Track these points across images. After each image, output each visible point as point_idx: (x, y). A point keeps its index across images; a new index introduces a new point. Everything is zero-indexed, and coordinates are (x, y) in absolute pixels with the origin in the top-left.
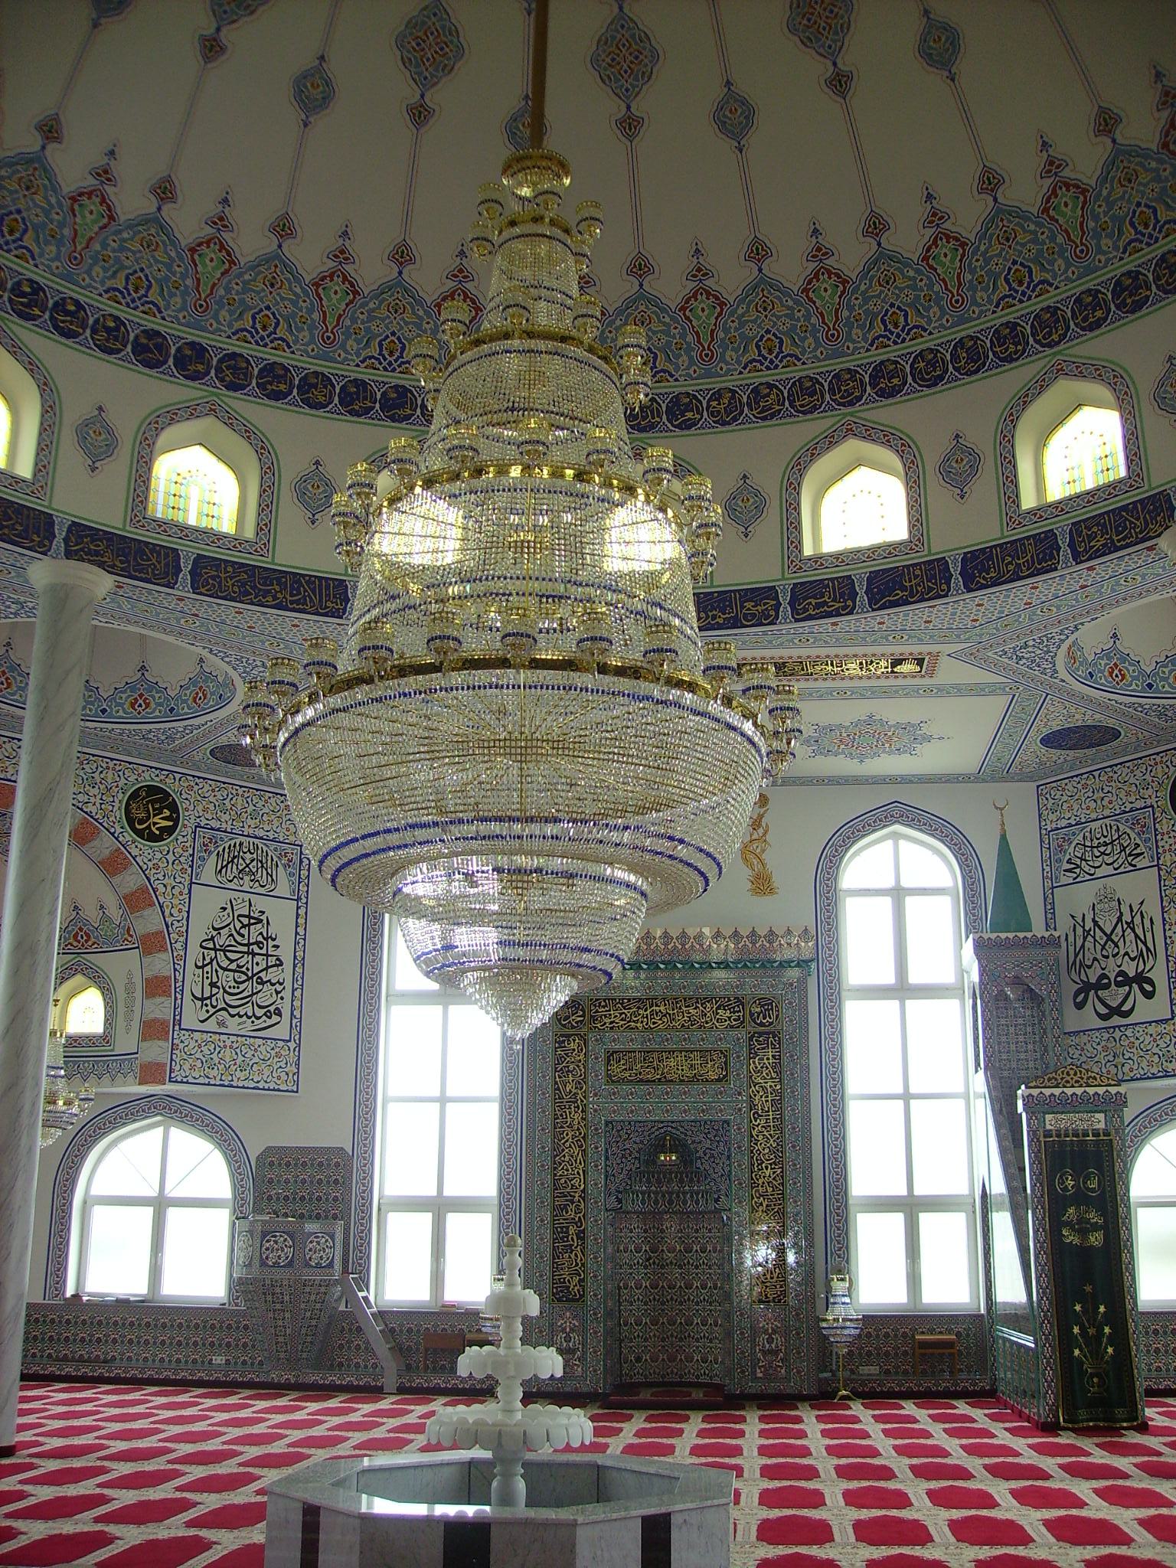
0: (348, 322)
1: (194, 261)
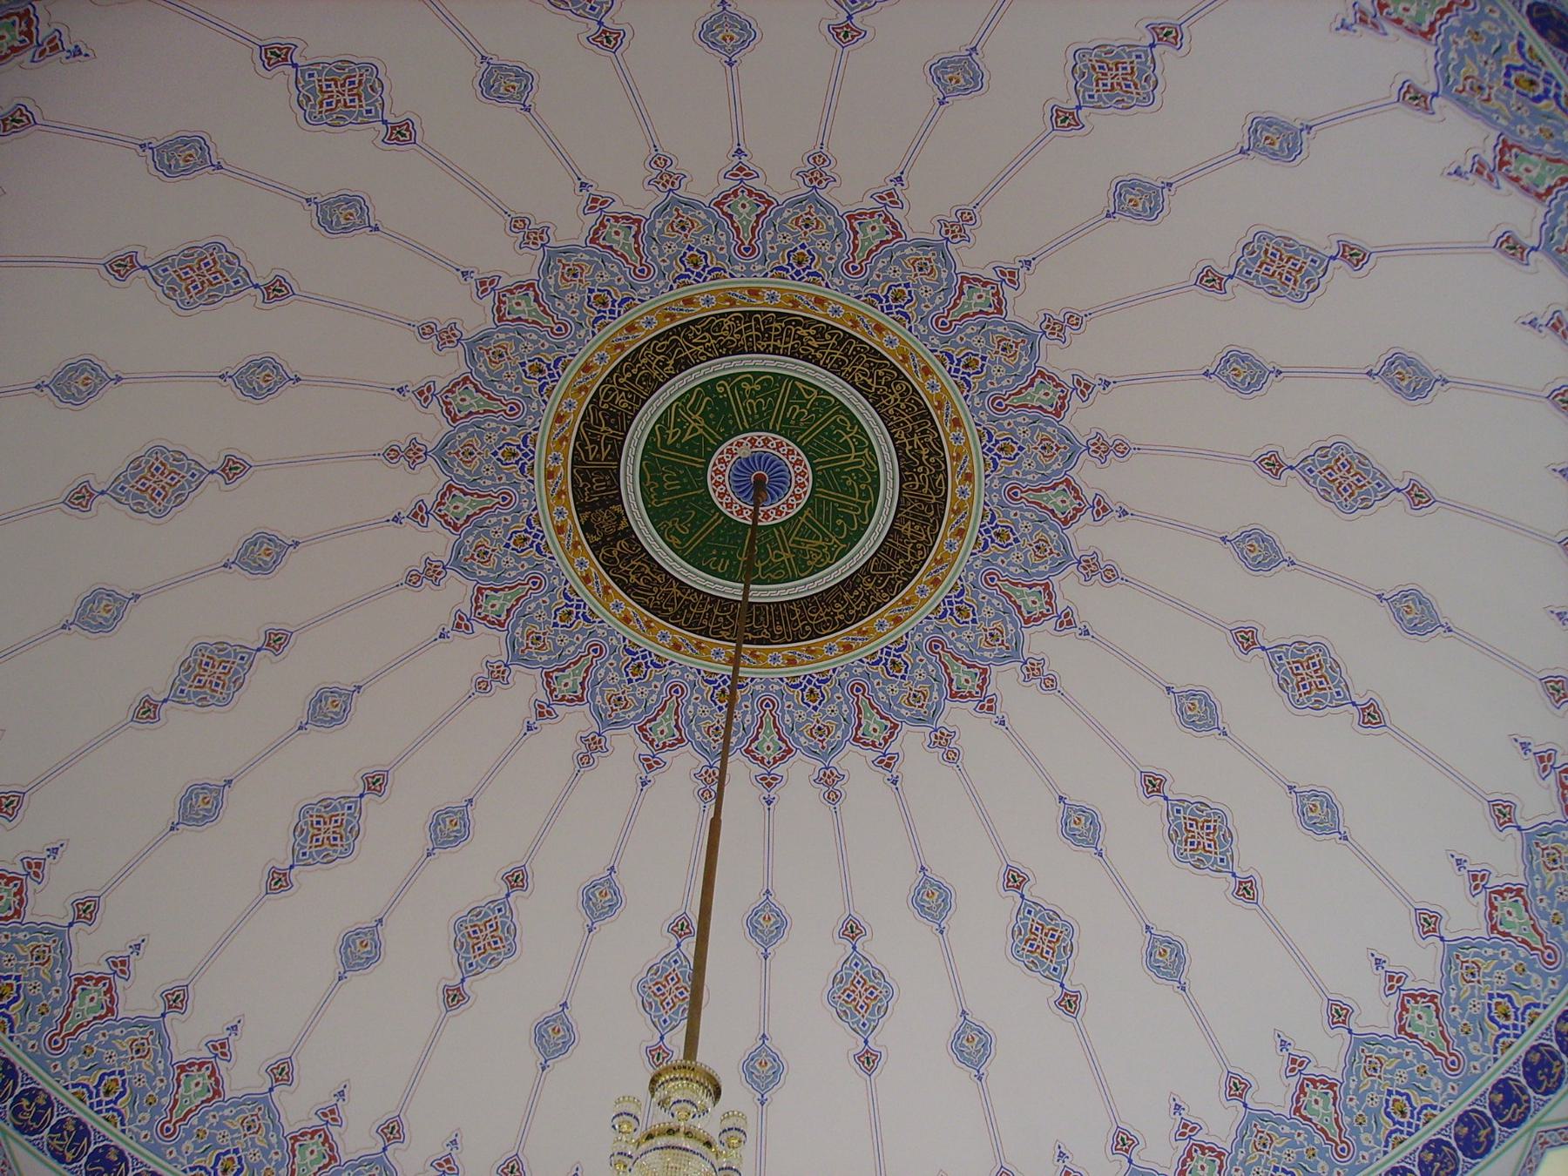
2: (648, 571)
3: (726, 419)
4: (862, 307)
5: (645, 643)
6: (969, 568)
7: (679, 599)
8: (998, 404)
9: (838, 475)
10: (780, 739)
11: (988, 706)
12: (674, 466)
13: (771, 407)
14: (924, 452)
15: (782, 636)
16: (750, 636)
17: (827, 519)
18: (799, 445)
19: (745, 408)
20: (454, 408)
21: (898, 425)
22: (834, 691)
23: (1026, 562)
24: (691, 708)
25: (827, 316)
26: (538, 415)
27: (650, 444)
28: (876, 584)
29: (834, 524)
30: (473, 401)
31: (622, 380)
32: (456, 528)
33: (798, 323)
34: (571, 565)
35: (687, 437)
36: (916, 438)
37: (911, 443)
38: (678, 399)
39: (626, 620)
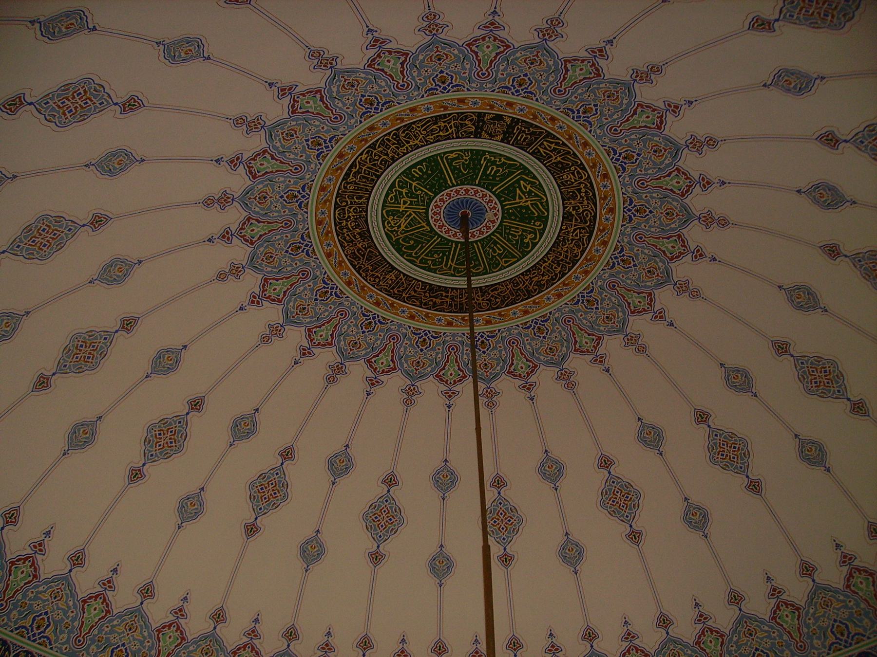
0: (805, 630)
1: (702, 649)
2: (441, 133)
3: (516, 216)
4: (545, 311)
7: (408, 142)
10: (267, 173)
11: (255, 300)
12: (504, 177)
13: (509, 240)
14: (438, 301)
15: (345, 188)
16: (354, 170)
17: (416, 236)
23: (348, 335)
25: (549, 293)
27: (526, 171)
28: (359, 250)
29: (411, 239)
31: (582, 186)
33: (552, 279)
35: (518, 191)
36: (449, 300)
37: (447, 297)
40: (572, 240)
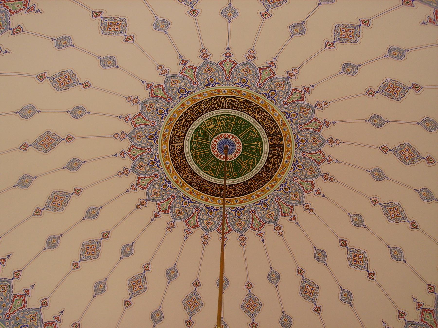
2: (264, 123)
4: (195, 199)
5: (268, 101)
6: (160, 126)
8: (156, 176)
9: (203, 148)
13: (222, 169)
14: (177, 157)
15: (222, 99)
16: (232, 99)
18: (214, 157)
19: (229, 168)
20: (311, 185)
21: (185, 165)
22: (204, 82)
23: (143, 131)
24: (255, 79)
25: (205, 196)
26: (289, 176)
28: (190, 116)
29: (204, 133)
30: (306, 185)
32: (321, 152)
33: (213, 194)
34: (289, 130)
37: (181, 160)
38: (248, 173)
39: (273, 110)
40: (236, 190)
